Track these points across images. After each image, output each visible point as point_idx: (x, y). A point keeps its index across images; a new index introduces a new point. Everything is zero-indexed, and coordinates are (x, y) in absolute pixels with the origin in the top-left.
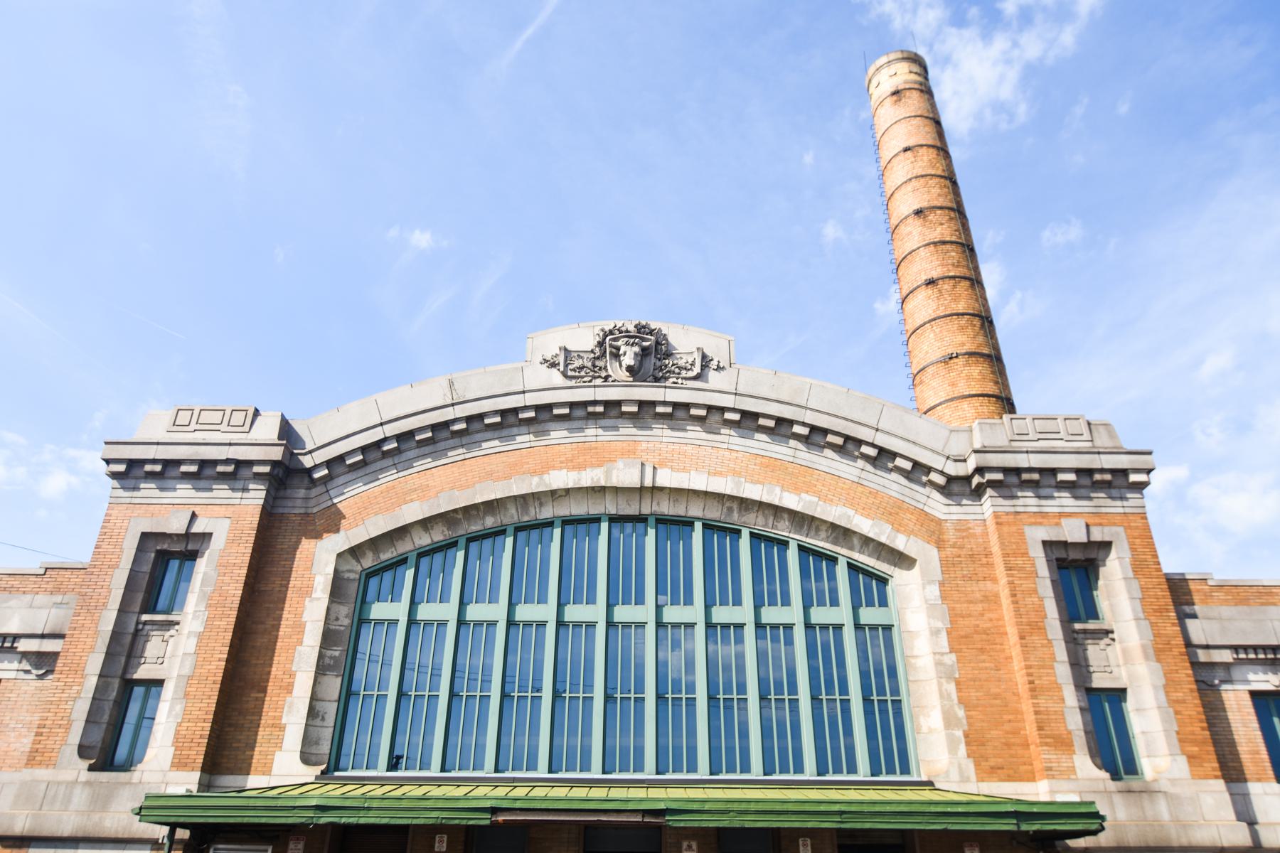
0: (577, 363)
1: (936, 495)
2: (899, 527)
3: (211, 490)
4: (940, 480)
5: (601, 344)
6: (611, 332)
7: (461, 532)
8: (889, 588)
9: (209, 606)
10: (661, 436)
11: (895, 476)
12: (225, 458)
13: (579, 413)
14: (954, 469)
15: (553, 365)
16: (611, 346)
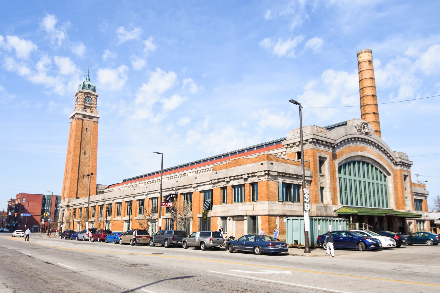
0: (359, 129)
1: (393, 164)
2: (390, 169)
3: (325, 148)
4: (394, 162)
5: (362, 125)
6: (363, 123)
8: (386, 178)
9: (330, 174)
10: (370, 148)
11: (389, 160)
12: (329, 142)
13: (363, 140)
14: (397, 161)
15: (356, 128)
16: (364, 126)
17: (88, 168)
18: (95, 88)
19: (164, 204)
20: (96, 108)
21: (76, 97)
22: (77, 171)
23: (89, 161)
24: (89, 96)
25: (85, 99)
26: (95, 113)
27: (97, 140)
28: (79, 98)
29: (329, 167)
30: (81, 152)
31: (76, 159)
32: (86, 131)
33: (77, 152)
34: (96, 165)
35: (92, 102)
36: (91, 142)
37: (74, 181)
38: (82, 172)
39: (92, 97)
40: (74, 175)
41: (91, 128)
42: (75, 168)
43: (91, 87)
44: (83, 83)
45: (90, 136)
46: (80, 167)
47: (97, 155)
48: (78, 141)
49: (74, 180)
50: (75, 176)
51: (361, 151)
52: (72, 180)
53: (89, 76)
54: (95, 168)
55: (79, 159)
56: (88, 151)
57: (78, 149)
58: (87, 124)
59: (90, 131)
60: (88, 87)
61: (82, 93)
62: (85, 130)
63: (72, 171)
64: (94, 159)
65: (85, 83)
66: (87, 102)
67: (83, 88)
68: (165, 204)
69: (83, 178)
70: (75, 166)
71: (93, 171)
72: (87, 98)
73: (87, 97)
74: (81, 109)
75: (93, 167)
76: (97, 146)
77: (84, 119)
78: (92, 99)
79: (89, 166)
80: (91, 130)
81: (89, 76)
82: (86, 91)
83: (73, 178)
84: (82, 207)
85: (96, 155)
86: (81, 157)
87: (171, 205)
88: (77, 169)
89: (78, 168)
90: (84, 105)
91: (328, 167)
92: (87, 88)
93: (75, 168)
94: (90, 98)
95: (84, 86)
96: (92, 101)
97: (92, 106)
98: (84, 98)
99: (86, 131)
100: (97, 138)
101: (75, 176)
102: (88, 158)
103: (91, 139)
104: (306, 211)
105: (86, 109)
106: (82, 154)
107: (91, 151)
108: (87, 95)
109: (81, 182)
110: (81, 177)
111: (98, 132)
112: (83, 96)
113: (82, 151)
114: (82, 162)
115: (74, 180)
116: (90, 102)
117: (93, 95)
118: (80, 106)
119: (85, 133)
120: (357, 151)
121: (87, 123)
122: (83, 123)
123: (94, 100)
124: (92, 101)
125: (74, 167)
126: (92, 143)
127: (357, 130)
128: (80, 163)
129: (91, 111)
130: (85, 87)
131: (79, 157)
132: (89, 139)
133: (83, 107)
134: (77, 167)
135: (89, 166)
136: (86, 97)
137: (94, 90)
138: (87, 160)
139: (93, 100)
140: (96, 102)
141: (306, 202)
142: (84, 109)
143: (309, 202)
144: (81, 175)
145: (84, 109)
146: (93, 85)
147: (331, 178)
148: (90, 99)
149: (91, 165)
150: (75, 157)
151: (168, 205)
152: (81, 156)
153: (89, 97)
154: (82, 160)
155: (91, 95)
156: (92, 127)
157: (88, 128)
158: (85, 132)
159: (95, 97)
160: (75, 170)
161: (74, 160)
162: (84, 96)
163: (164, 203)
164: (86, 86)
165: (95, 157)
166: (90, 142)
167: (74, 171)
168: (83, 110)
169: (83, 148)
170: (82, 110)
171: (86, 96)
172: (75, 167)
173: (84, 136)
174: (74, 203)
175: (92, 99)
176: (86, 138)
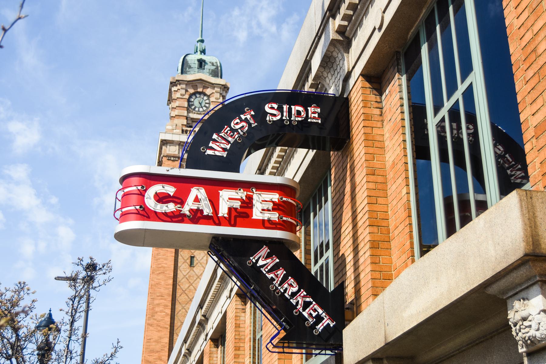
18: (217, 67)
19: (161, 198)
22: (168, 319)
24: (200, 90)
25: (189, 101)
30: (180, 257)
31: (163, 283)
33: (166, 259)
39: (208, 91)
40: (155, 335)
42: (161, 312)
43: (208, 67)
49: (157, 352)
50: (161, 338)
52: (152, 351)
53: (202, 41)
55: (171, 282)
61: (180, 84)
63: (150, 322)
65: (188, 58)
66: (194, 109)
68: (180, 200)
70: (158, 305)
72: (194, 97)
73: (194, 94)
78: (209, 96)
81: (202, 41)
82: (189, 77)
83: (154, 346)
87: (257, 214)
88: (167, 314)
89: (169, 311)
90: (187, 118)
92: (196, 70)
93: (161, 312)
94: (205, 95)
96: (209, 104)
98: (187, 96)
101: (161, 338)
108: (195, 87)
112: (183, 92)
115: (157, 352)
116: (205, 108)
117: (213, 85)
118: (176, 121)
123: (217, 99)
124: (209, 104)
128: (178, 295)
130: (190, 67)
131: (172, 275)
133: (185, 122)
134: (166, 306)
136: (191, 96)
137: (217, 72)
139: (212, 99)
142: (185, 128)
145: (185, 128)
148: (205, 98)
150: (161, 276)
151: (223, 211)
152: (179, 272)
153: (200, 93)
155: (208, 88)
159: (218, 90)
160: (160, 318)
161: (158, 284)
162: (186, 91)
163: (158, 188)
164: (192, 66)
167: (155, 322)
168: (183, 131)
171: (191, 91)
172: (161, 308)
175: (209, 96)
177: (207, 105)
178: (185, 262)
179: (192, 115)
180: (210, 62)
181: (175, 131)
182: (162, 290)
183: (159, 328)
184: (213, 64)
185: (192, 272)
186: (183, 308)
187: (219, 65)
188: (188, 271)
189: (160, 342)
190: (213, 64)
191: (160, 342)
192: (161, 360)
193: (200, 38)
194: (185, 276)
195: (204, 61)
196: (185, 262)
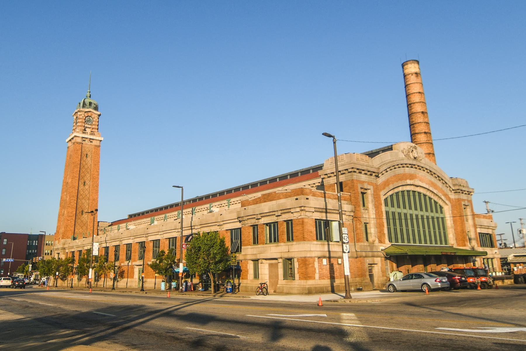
0: (406, 153)
7: (395, 192)
9: (375, 207)
17: (88, 201)
18: (96, 106)
20: (98, 129)
21: (75, 117)
23: (89, 193)
26: (97, 135)
27: (98, 167)
28: (78, 118)
29: (373, 199)
31: (74, 191)
32: (87, 156)
34: (97, 198)
35: (94, 123)
36: (92, 170)
37: (71, 218)
38: (80, 206)
41: (92, 153)
43: (93, 105)
44: (83, 100)
45: (91, 163)
46: (79, 200)
47: (98, 186)
48: (77, 170)
49: (72, 216)
50: (73, 212)
51: (410, 179)
52: (70, 216)
54: (96, 201)
56: (88, 181)
57: (76, 178)
58: (87, 149)
59: (91, 157)
60: (89, 105)
62: (85, 155)
64: (95, 191)
65: (85, 101)
66: (87, 123)
67: (83, 107)
69: (82, 214)
70: (72, 199)
71: (93, 205)
74: (80, 131)
75: (94, 200)
76: (98, 175)
77: (83, 142)
79: (89, 199)
80: (92, 155)
83: (70, 214)
84: (82, 249)
85: (97, 186)
86: (80, 189)
91: (372, 199)
92: (88, 106)
95: (84, 103)
97: (94, 127)
98: (85, 118)
99: (87, 156)
100: (99, 165)
101: (73, 212)
102: (88, 190)
103: (92, 166)
104: (345, 253)
105: (86, 131)
106: (81, 185)
107: (91, 182)
109: (79, 218)
110: (80, 212)
111: (99, 158)
113: (80, 181)
114: (81, 195)
116: (91, 123)
118: (80, 128)
119: (84, 159)
120: (406, 180)
121: (87, 147)
122: (83, 148)
123: (96, 120)
124: (93, 121)
125: (71, 201)
126: (93, 171)
127: (405, 156)
128: (79, 196)
129: (92, 133)
130: (86, 105)
132: (90, 167)
134: (75, 200)
135: (89, 199)
138: (87, 192)
139: (94, 120)
140: (98, 122)
141: (345, 243)
142: (83, 131)
143: (348, 242)
144: (79, 210)
146: (95, 103)
147: (376, 212)
148: (91, 119)
149: (91, 198)
150: (74, 189)
154: (82, 193)
156: (93, 152)
157: (88, 153)
158: (85, 158)
160: (72, 204)
165: (96, 188)
166: (91, 170)
169: (83, 178)
170: (81, 132)
173: (84, 163)
174: (71, 245)
176: (86, 166)
177: (92, 122)
178: (82, 184)
179: (86, 126)
180: (94, 103)
181: (80, 132)
182: (74, 194)
183: (72, 208)
184: (95, 105)
185: (84, 188)
186: (81, 201)
187: (97, 105)
188: (83, 187)
189: (72, 213)
190: (95, 105)
191: (72, 213)
192: (72, 219)
193: (89, 91)
194: (82, 189)
195: (92, 103)
196: (82, 184)
